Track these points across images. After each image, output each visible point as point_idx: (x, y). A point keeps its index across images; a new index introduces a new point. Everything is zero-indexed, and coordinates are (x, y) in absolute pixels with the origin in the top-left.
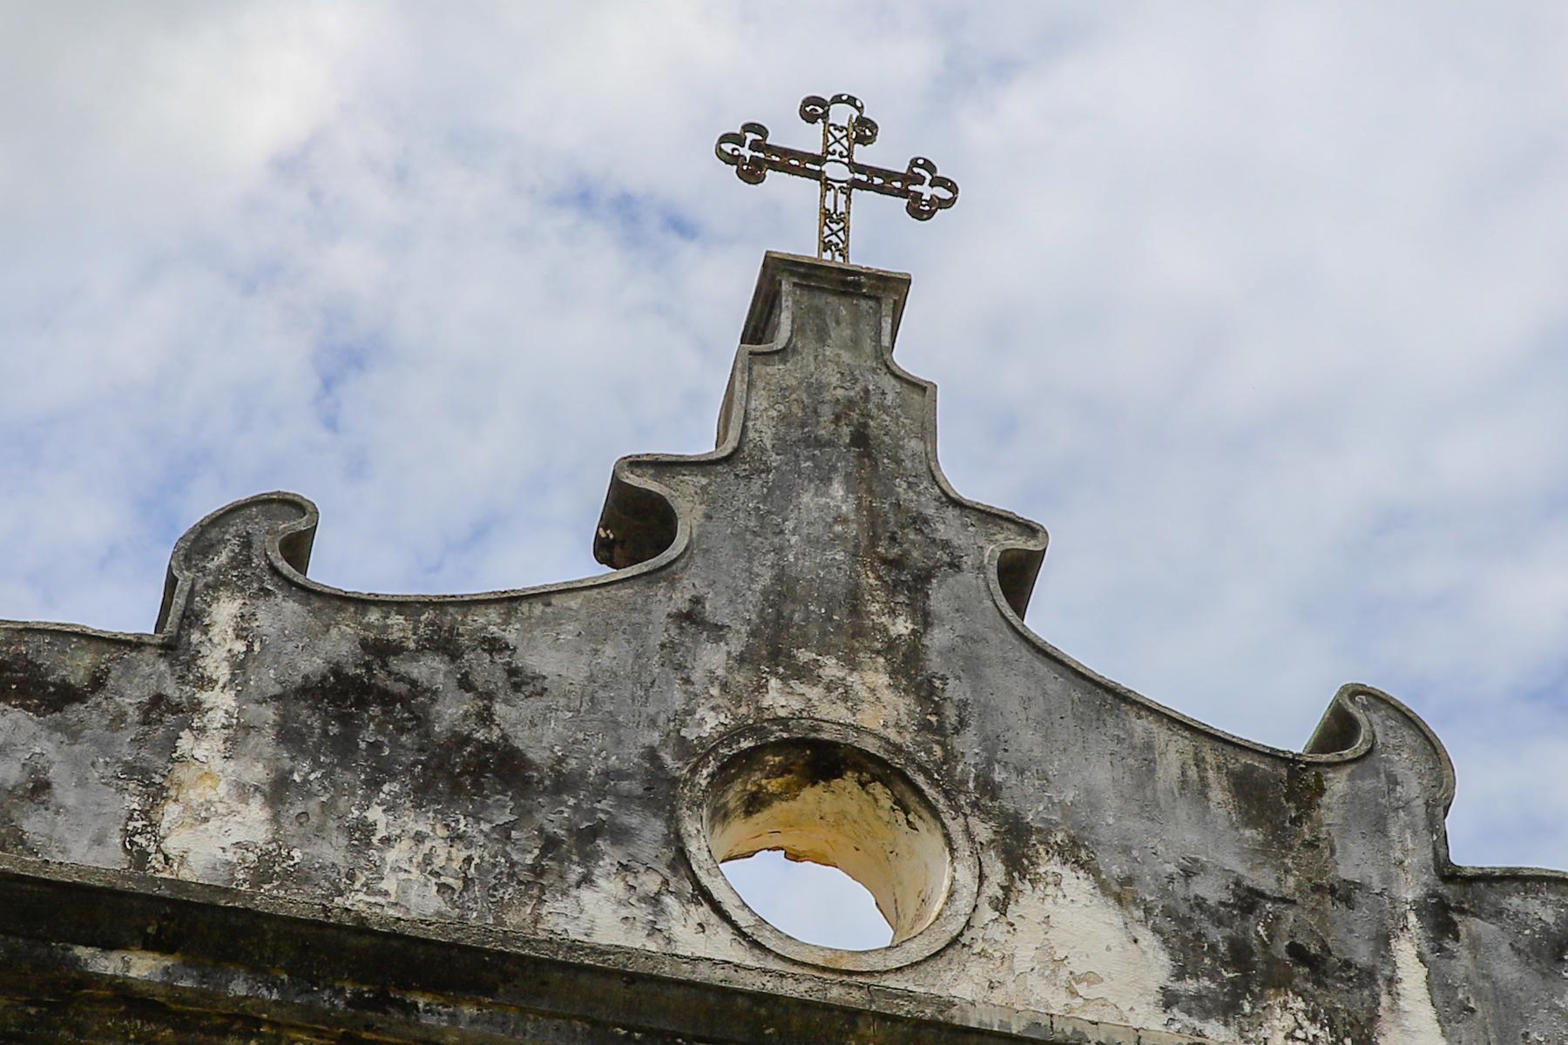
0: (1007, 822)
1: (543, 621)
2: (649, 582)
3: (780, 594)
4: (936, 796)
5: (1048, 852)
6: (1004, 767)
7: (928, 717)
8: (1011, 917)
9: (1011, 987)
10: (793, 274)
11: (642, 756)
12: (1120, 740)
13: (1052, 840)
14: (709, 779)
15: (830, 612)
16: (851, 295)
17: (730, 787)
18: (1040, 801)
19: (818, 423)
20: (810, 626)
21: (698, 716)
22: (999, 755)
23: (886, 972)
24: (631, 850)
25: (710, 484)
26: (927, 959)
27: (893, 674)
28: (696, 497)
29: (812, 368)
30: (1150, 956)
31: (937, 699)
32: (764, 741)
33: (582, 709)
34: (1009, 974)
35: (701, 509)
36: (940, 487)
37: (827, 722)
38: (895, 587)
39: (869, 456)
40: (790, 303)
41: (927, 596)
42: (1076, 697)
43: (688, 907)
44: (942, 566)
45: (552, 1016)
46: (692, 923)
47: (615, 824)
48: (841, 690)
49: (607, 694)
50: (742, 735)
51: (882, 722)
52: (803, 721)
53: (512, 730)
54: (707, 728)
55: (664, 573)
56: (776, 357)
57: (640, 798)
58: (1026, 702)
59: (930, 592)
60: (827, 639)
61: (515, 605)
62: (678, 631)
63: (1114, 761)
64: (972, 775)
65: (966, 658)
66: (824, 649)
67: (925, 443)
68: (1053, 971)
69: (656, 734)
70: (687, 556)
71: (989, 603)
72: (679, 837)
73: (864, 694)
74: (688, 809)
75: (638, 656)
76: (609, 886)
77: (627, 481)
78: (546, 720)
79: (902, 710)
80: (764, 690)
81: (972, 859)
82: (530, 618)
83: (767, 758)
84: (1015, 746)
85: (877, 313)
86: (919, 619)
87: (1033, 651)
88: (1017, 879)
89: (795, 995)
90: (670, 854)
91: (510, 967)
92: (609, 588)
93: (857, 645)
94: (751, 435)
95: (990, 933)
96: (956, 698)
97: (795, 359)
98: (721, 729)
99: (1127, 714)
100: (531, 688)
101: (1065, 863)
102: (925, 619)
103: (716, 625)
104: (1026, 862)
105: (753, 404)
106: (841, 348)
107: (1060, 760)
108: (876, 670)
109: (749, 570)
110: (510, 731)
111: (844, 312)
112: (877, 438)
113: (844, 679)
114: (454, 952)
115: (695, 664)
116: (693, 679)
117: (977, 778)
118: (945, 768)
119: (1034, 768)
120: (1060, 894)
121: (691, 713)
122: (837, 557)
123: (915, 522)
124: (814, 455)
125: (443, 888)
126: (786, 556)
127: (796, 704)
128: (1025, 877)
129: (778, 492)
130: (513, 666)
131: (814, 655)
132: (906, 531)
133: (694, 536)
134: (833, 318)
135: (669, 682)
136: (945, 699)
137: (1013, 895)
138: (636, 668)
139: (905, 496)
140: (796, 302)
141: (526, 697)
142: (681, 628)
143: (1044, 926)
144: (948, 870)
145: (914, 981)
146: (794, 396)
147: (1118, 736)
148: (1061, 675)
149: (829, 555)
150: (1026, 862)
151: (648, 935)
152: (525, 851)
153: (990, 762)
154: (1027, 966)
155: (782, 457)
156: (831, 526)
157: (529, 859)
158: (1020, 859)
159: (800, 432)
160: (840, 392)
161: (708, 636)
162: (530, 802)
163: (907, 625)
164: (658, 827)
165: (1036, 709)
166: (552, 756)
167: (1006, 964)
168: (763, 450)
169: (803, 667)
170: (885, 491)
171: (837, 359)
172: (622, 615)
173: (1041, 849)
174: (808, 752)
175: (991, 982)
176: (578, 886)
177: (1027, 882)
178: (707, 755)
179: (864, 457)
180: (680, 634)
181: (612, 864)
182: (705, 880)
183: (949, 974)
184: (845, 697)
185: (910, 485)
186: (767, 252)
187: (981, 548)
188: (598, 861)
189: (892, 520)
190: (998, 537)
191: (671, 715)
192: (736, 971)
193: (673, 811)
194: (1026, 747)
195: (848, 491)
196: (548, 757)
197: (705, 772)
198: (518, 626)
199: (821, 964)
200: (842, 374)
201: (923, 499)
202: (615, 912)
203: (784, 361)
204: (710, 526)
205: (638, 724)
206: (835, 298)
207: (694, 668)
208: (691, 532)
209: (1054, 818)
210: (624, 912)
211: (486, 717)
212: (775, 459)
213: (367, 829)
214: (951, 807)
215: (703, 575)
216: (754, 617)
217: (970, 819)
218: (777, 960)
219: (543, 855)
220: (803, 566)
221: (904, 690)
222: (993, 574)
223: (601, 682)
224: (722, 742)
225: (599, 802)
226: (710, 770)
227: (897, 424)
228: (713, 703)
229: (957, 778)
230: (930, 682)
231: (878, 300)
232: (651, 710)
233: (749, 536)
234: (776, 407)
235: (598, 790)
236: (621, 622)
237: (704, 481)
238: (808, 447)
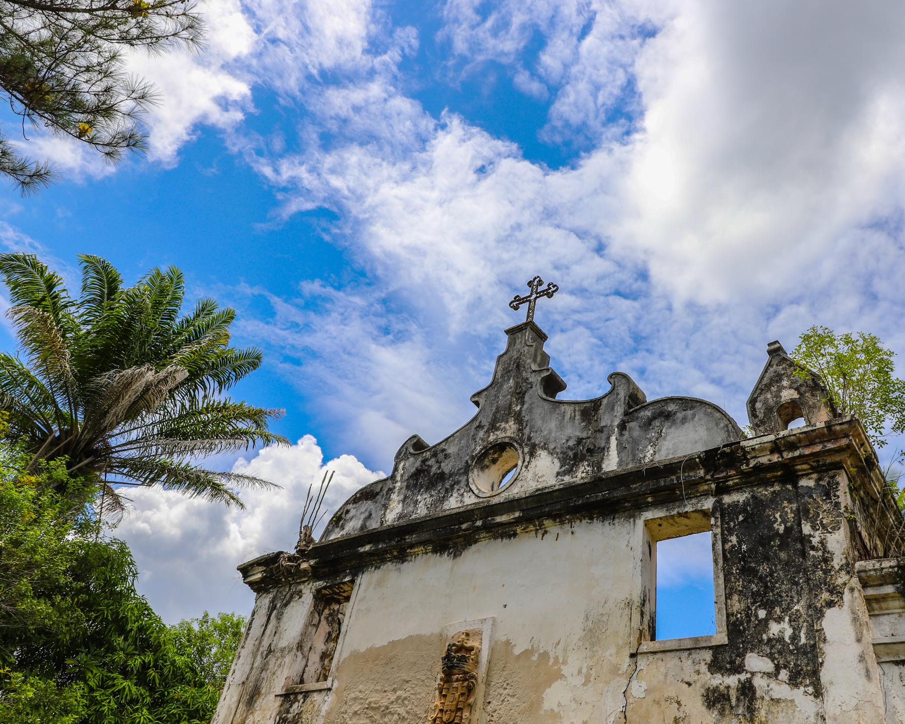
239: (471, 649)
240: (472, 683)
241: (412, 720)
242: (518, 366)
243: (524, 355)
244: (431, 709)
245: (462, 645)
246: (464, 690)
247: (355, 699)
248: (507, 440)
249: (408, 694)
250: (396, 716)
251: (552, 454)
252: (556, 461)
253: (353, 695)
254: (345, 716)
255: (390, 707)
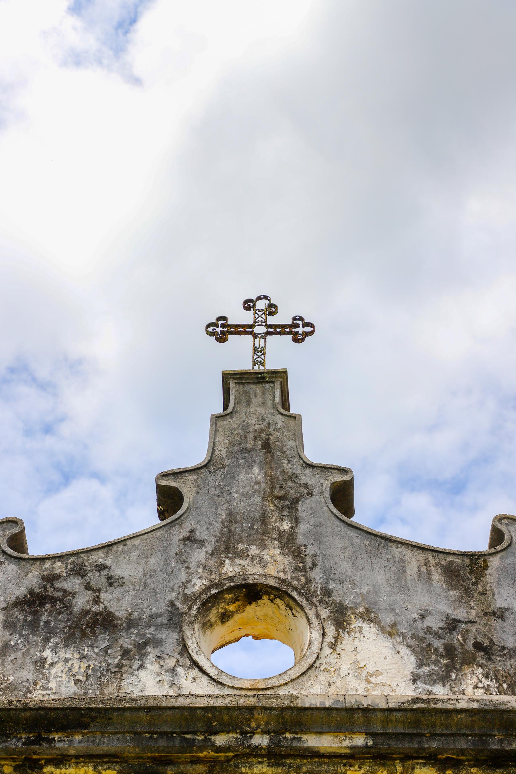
0: (336, 607)
1: (123, 553)
2: (170, 527)
3: (230, 521)
4: (301, 600)
5: (356, 617)
6: (334, 581)
7: (299, 565)
8: (338, 650)
9: (339, 684)
10: (234, 379)
11: (168, 606)
12: (388, 560)
13: (357, 611)
14: (197, 611)
15: (253, 525)
16: (262, 383)
17: (210, 613)
18: (351, 594)
19: (247, 442)
20: (244, 533)
21: (192, 583)
22: (331, 577)
23: (280, 686)
24: (162, 649)
25: (198, 478)
26: (298, 677)
27: (282, 548)
28: (192, 485)
29: (244, 418)
30: (406, 658)
31: (302, 556)
32: (222, 589)
33: (140, 589)
34: (338, 678)
35: (194, 490)
36: (302, 460)
37: (251, 575)
38: (282, 508)
39: (270, 452)
40: (234, 392)
41: (297, 510)
42: (367, 544)
43: (188, 671)
44: (304, 495)
45: (116, 733)
46: (190, 678)
47: (155, 639)
48: (258, 559)
49: (151, 580)
50: (212, 588)
51: (277, 571)
52: (240, 577)
53: (109, 604)
54: (197, 588)
55: (178, 521)
56: (228, 417)
57: (166, 624)
58: (344, 550)
59: (298, 508)
60: (251, 537)
61: (110, 548)
62: (183, 546)
63: (386, 570)
64: (319, 588)
65: (315, 535)
66: (250, 542)
67: (296, 442)
68: (359, 673)
69: (174, 594)
70: (188, 512)
71: (326, 508)
72: (183, 640)
73: (269, 559)
74: (187, 626)
75: (165, 561)
76: (152, 667)
77: (161, 484)
78: (124, 597)
79: (286, 563)
80: (223, 566)
81: (319, 627)
82: (117, 552)
83: (225, 596)
84: (339, 571)
85: (273, 388)
86: (294, 521)
87: (347, 526)
88: (341, 632)
89: (224, 705)
90: (180, 648)
91: (93, 714)
92: (153, 533)
93: (265, 538)
94: (217, 453)
95: (328, 660)
96: (311, 554)
97: (236, 416)
98: (203, 587)
99: (391, 547)
100: (117, 584)
101: (364, 621)
102: (296, 520)
103: (201, 540)
104: (345, 624)
105: (217, 439)
106: (257, 407)
107: (360, 574)
108: (274, 548)
109: (216, 513)
110: (107, 604)
111: (259, 391)
112: (273, 443)
113: (259, 554)
114: (68, 712)
115: (191, 560)
116: (190, 567)
117: (321, 588)
118: (306, 586)
119: (348, 579)
120: (362, 636)
121: (189, 582)
122: (256, 500)
123: (291, 478)
124: (245, 456)
125: (77, 681)
126: (233, 503)
127: (237, 569)
128: (345, 631)
129: (229, 476)
130: (110, 575)
131: (245, 546)
132: (287, 482)
133: (191, 502)
134: (254, 394)
135: (179, 570)
136: (306, 555)
137: (339, 641)
138: (165, 567)
139: (287, 467)
140: (237, 391)
141: (115, 588)
142: (185, 544)
143: (355, 652)
144: (309, 633)
145: (293, 688)
146: (236, 432)
147: (388, 558)
148: (359, 535)
149: (252, 500)
150: (345, 624)
151: (170, 687)
152: (114, 658)
153: (327, 581)
154: (346, 673)
155: (230, 460)
156: (253, 487)
157: (116, 662)
158: (343, 623)
159: (238, 447)
160: (257, 427)
161: (197, 546)
162: (117, 635)
163: (288, 524)
164: (175, 636)
165: (348, 553)
166: (127, 612)
167: (336, 673)
168: (222, 459)
169: (240, 552)
170: (278, 466)
171: (255, 412)
172: (158, 544)
173: (353, 617)
174: (244, 590)
175: (330, 683)
176: (138, 670)
177: (346, 633)
178: (196, 600)
179: (267, 453)
180: (184, 547)
181: (153, 657)
182: (195, 657)
183: (309, 682)
184: (260, 562)
185: (289, 462)
186: (222, 371)
187: (322, 484)
188: (147, 657)
189: (281, 478)
190: (329, 477)
191: (180, 584)
192: (196, 698)
193: (181, 628)
194: (344, 570)
195: (260, 469)
196: (125, 613)
197: (195, 608)
198: (112, 557)
199: (249, 686)
200: (258, 418)
201: (295, 467)
202: (154, 679)
203: (231, 417)
204: (198, 497)
205: (166, 591)
206: (254, 385)
207: (191, 561)
208: (190, 502)
209: (358, 601)
210: (159, 678)
211: (97, 601)
212: (227, 462)
213: (42, 661)
214: (309, 604)
215: (195, 519)
216: (218, 534)
217: (319, 608)
218: (229, 689)
219: (122, 658)
220: (240, 507)
221: (287, 554)
222: (327, 495)
223: (149, 575)
224: (203, 593)
225: (148, 629)
226: (197, 606)
227: (283, 436)
228: (199, 575)
229: (312, 590)
230: (299, 548)
231: (273, 382)
232: (171, 584)
233: (216, 498)
234: (228, 438)
235: (147, 624)
236: (158, 547)
237: (195, 477)
238: (242, 453)
242: (267, 446)
243: (276, 430)
248: (271, 582)
251: (390, 634)
252: (404, 650)
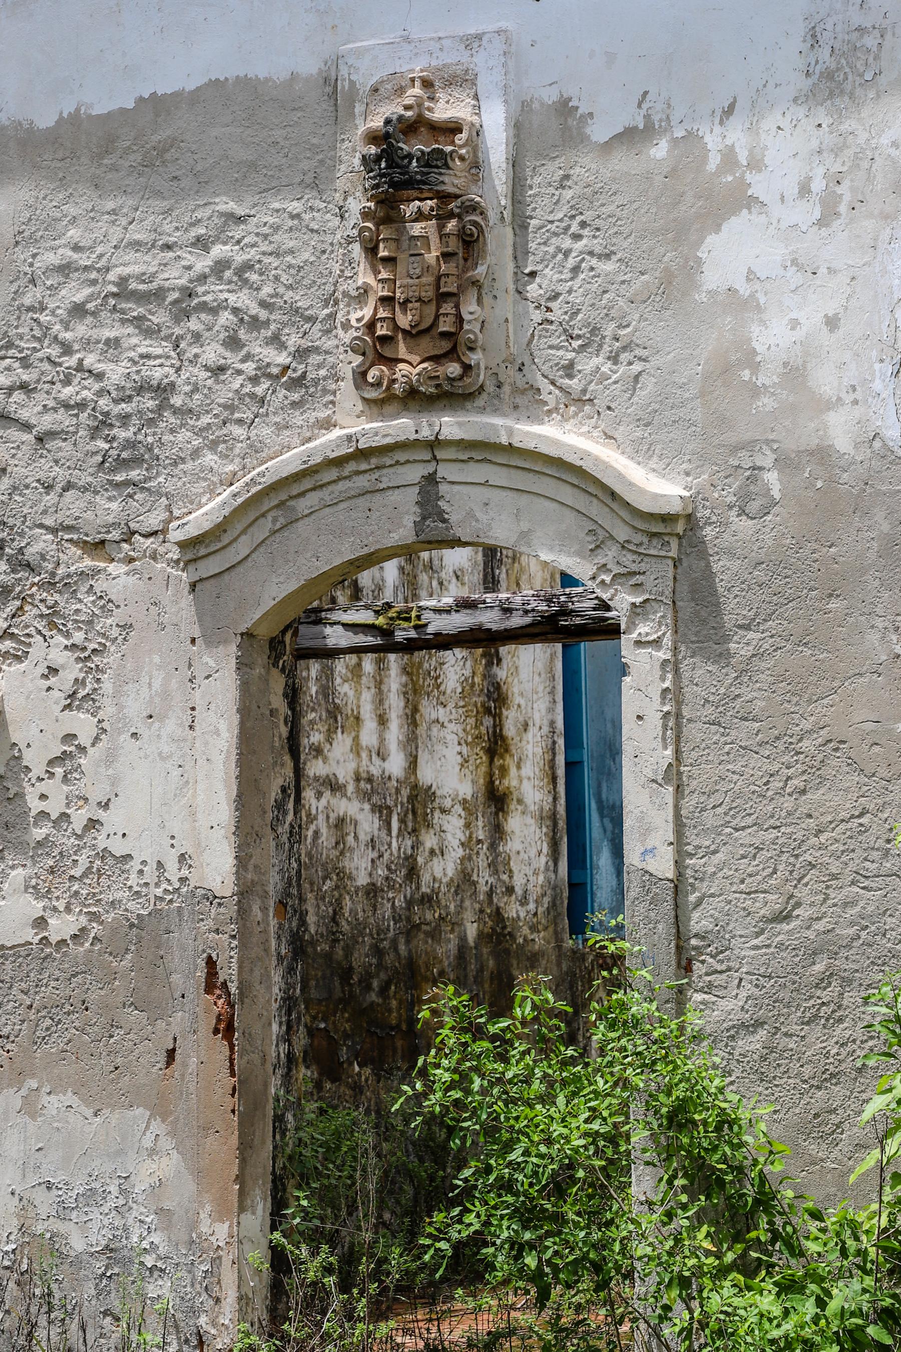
239: (452, 129)
240: (475, 224)
241: (285, 325)
244: (345, 294)
245: (420, 116)
246: (454, 245)
247: (65, 269)
249: (252, 254)
250: (225, 317)
253: (51, 259)
254: (44, 318)
255: (200, 290)
